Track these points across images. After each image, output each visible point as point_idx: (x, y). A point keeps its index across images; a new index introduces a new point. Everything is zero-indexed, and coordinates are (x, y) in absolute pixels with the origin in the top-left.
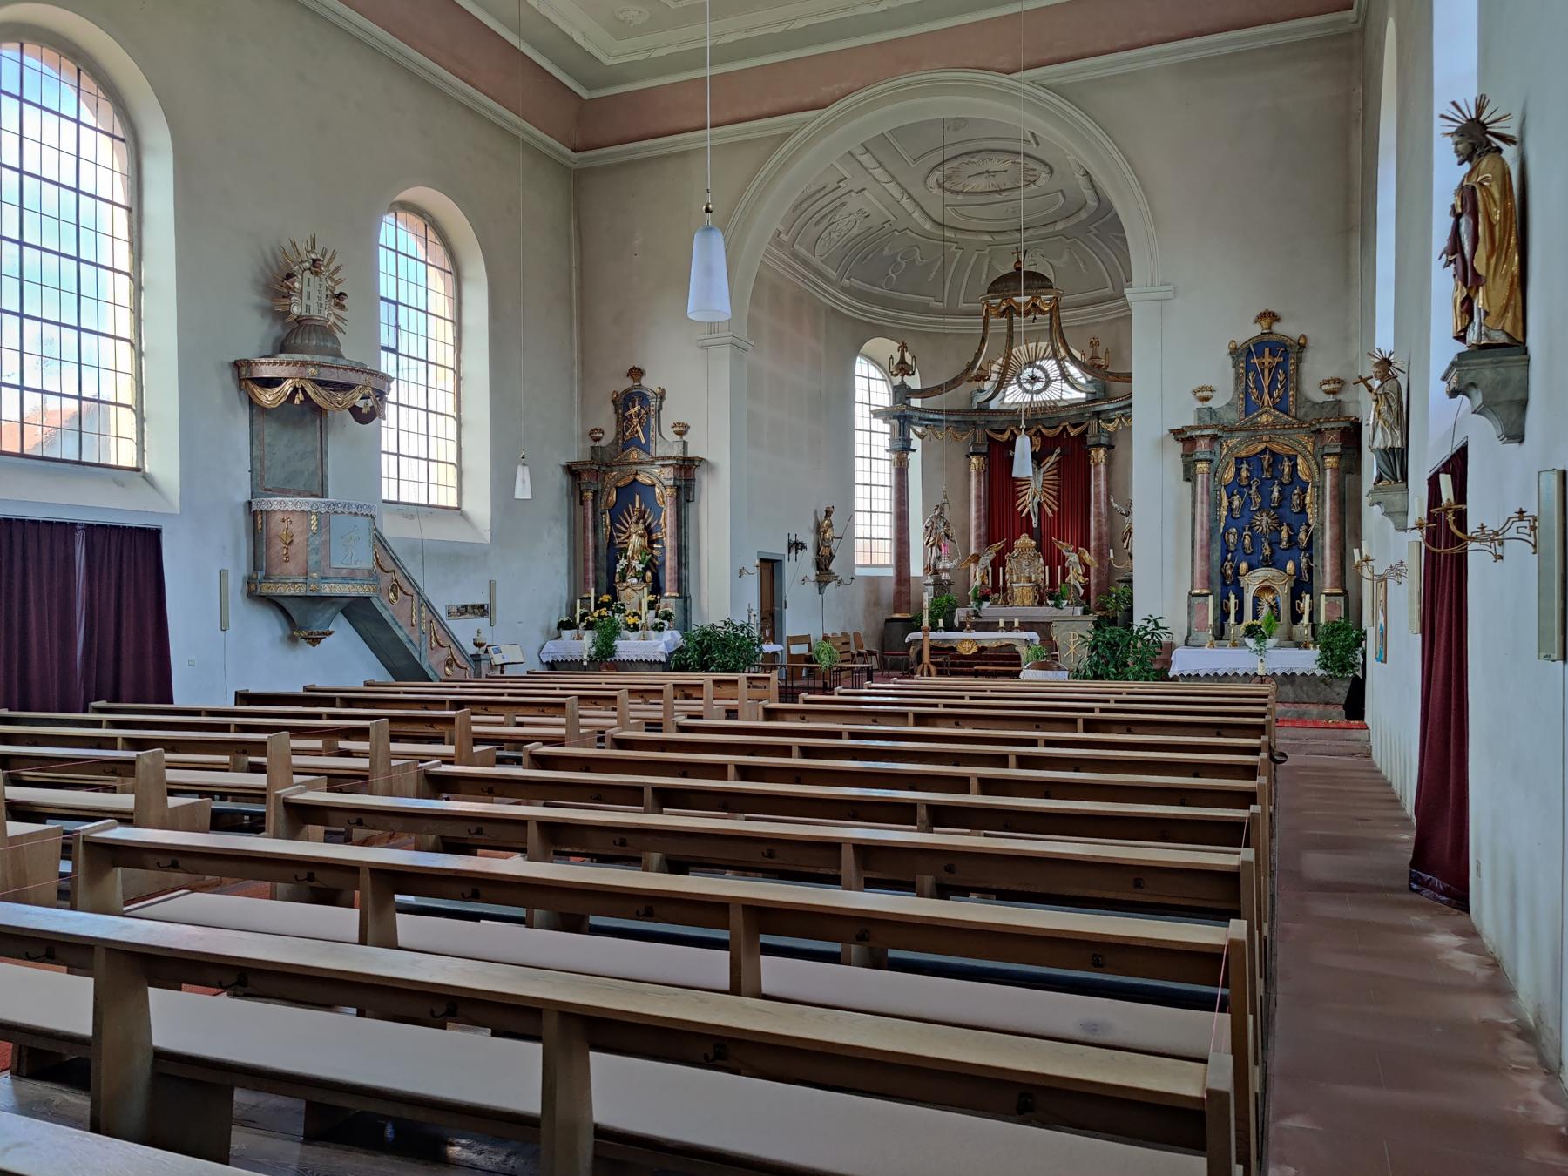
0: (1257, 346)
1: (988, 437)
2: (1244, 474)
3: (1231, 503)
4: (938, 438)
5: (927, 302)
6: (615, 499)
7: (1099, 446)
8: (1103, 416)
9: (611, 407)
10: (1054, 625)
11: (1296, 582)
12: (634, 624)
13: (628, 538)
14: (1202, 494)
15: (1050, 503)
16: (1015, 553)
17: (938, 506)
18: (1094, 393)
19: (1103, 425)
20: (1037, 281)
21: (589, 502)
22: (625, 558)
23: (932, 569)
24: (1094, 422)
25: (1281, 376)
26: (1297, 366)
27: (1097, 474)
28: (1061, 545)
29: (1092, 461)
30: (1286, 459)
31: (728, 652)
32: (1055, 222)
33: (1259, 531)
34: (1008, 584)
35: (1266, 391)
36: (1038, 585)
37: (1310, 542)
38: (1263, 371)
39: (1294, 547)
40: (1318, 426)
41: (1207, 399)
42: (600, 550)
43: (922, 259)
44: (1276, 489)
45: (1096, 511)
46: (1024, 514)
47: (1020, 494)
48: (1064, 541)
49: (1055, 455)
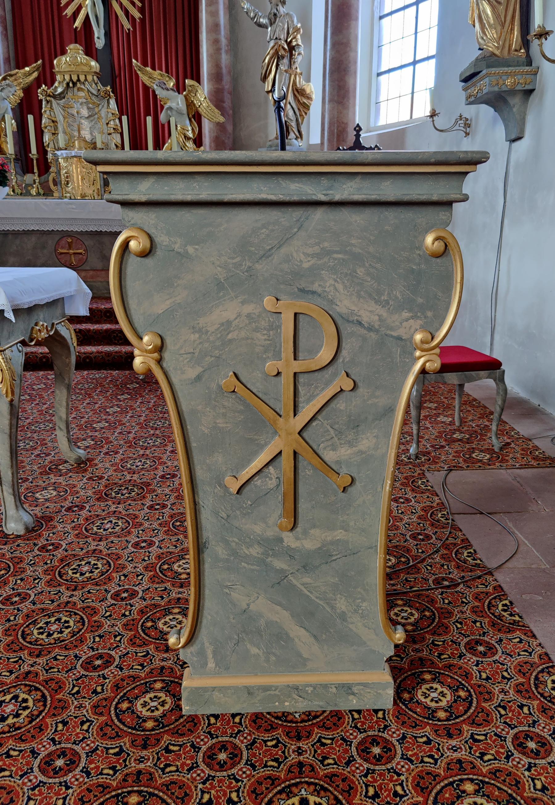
46: (78, 23)
48: (154, 68)
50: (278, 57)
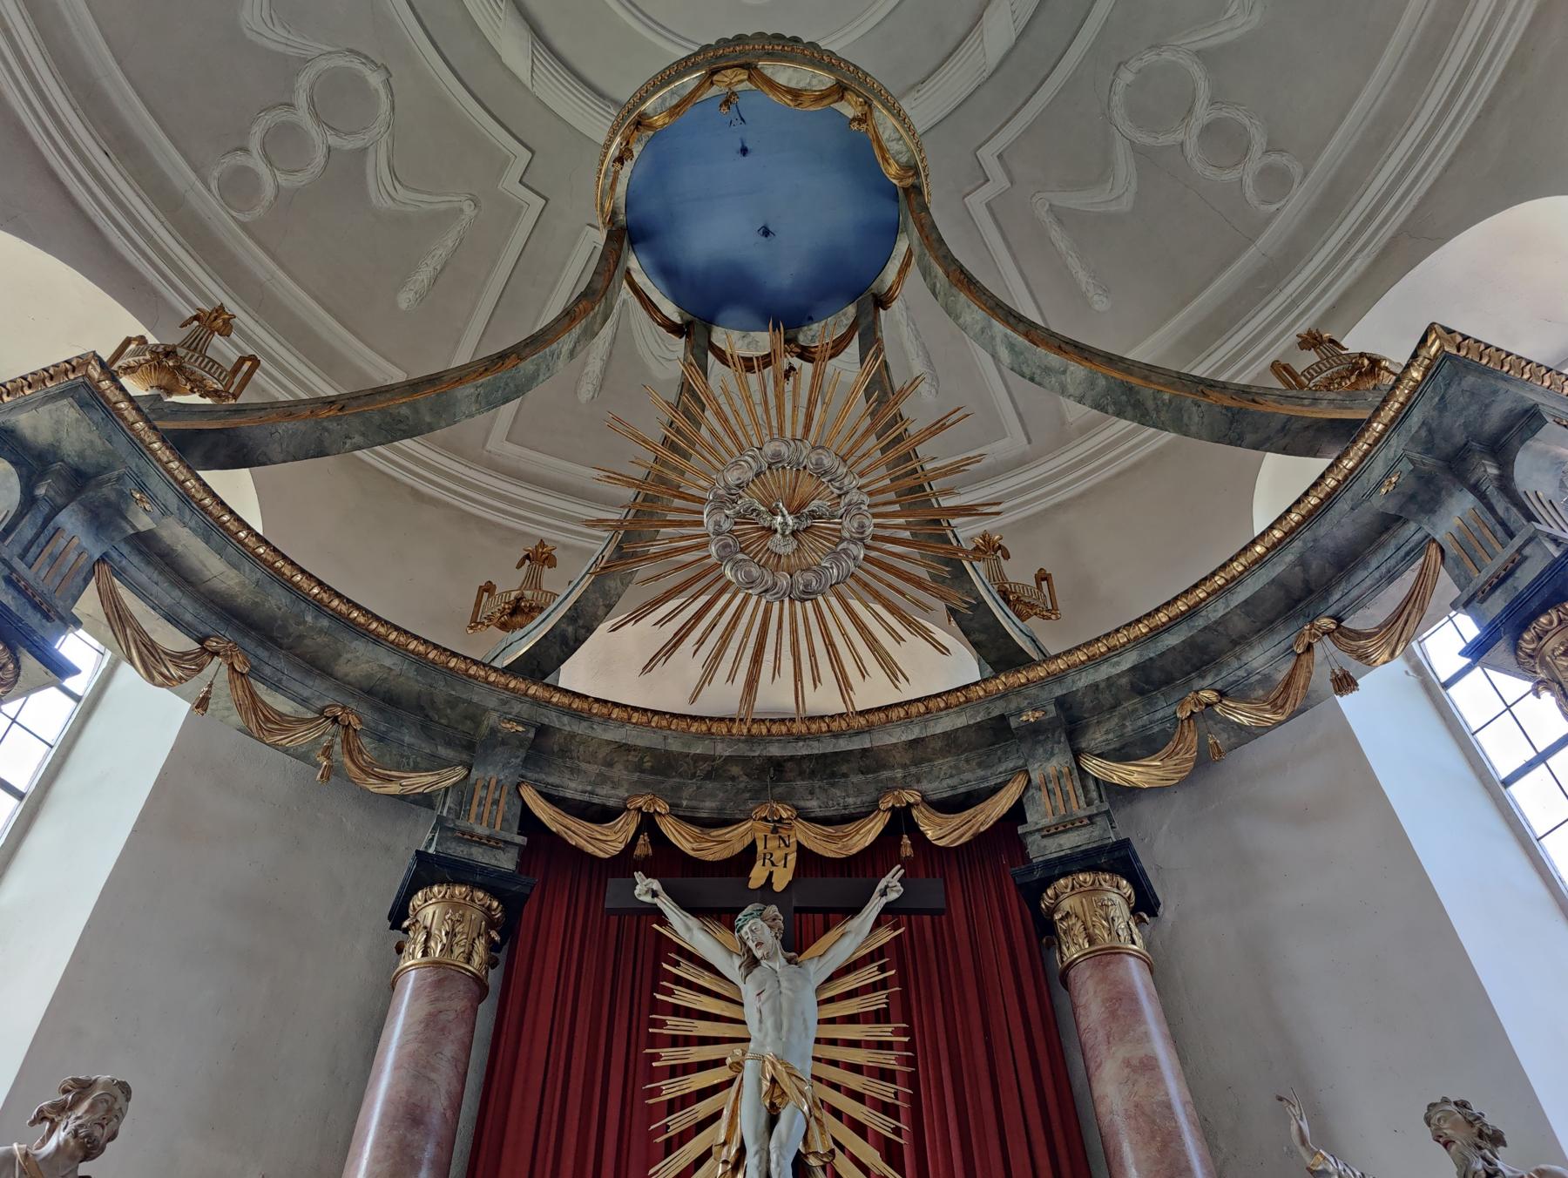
1: (528, 821)
8: (1097, 737)
17: (83, 1088)
47: (678, 1122)
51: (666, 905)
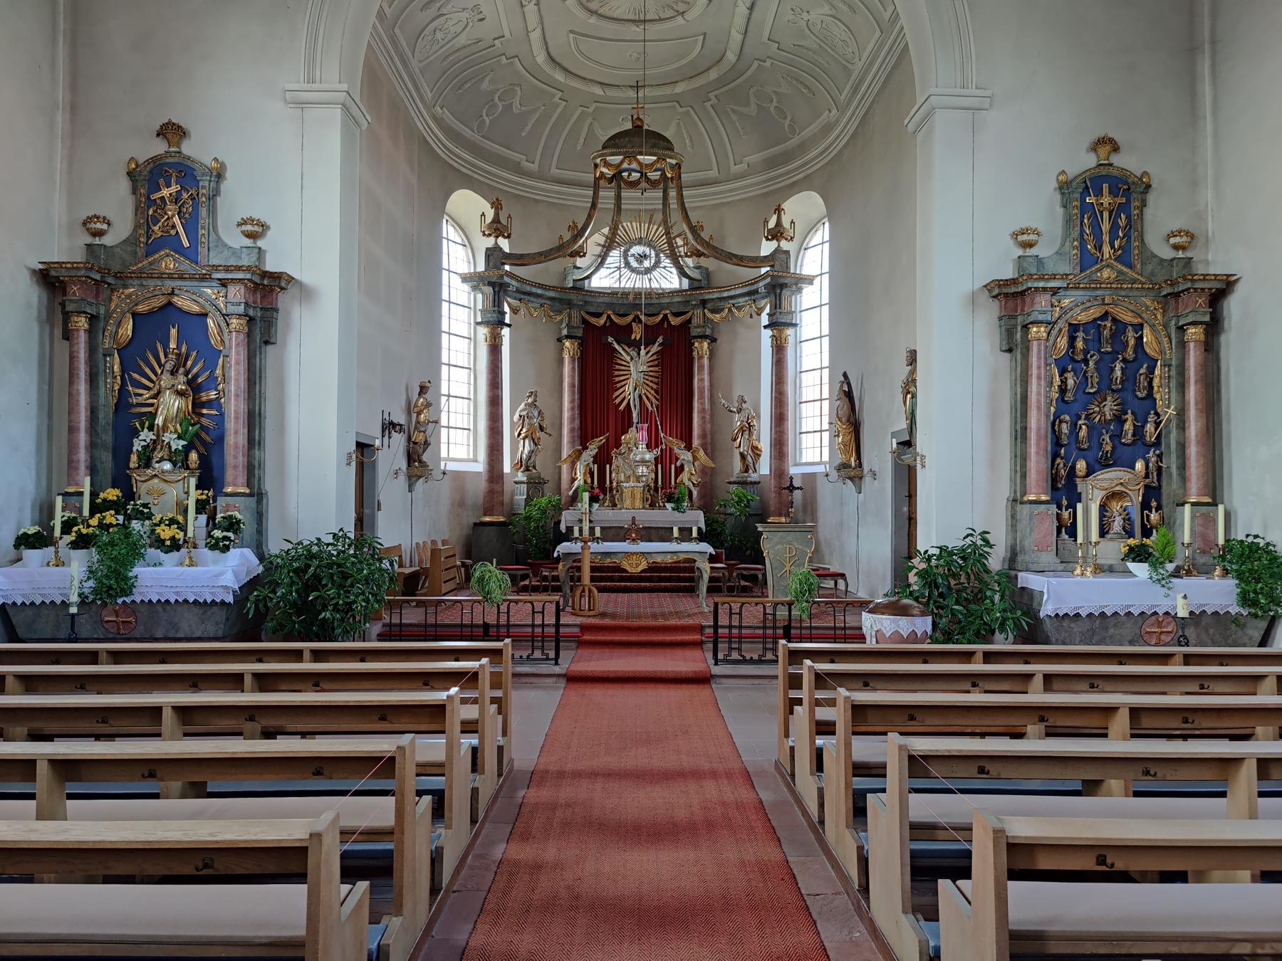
0: (1092, 182)
1: (584, 321)
2: (1080, 344)
3: (1064, 382)
4: (532, 315)
5: (518, 160)
6: (130, 333)
7: (704, 337)
8: (709, 305)
9: (124, 185)
10: (764, 536)
11: (1146, 487)
12: (173, 539)
13: (156, 396)
14: (1039, 367)
15: (650, 396)
16: (623, 449)
17: (532, 392)
18: (700, 280)
19: (709, 315)
20: (659, 142)
21: (82, 334)
22: (151, 428)
23: (526, 465)
24: (699, 311)
25: (1122, 221)
26: (1142, 211)
27: (701, 367)
28: (670, 442)
29: (695, 354)
30: (1130, 328)
31: (352, 585)
32: (677, 82)
33: (1097, 419)
34: (615, 484)
35: (1106, 238)
36: (648, 485)
37: (1159, 437)
38: (1101, 213)
39: (1139, 442)
40: (1189, 285)
41: (1030, 245)
42: (101, 415)
43: (520, 104)
44: (1118, 367)
45: (701, 407)
46: (622, 408)
47: (618, 385)
49: (657, 344)
50: (742, 430)
51: (614, 343)
